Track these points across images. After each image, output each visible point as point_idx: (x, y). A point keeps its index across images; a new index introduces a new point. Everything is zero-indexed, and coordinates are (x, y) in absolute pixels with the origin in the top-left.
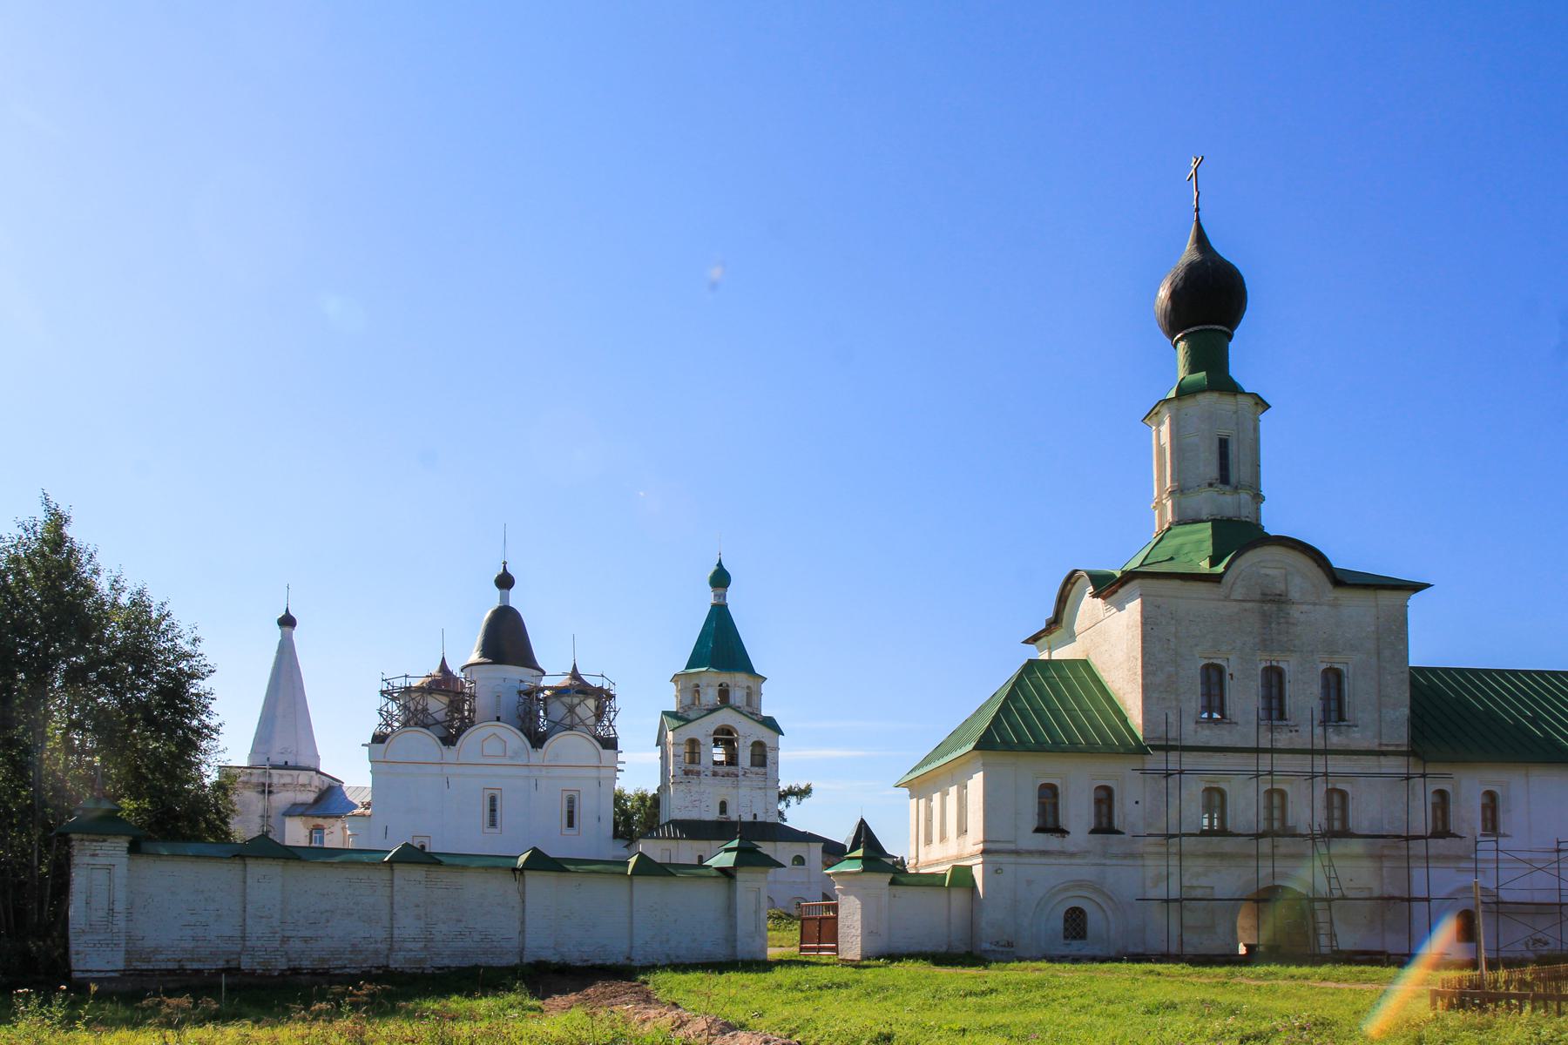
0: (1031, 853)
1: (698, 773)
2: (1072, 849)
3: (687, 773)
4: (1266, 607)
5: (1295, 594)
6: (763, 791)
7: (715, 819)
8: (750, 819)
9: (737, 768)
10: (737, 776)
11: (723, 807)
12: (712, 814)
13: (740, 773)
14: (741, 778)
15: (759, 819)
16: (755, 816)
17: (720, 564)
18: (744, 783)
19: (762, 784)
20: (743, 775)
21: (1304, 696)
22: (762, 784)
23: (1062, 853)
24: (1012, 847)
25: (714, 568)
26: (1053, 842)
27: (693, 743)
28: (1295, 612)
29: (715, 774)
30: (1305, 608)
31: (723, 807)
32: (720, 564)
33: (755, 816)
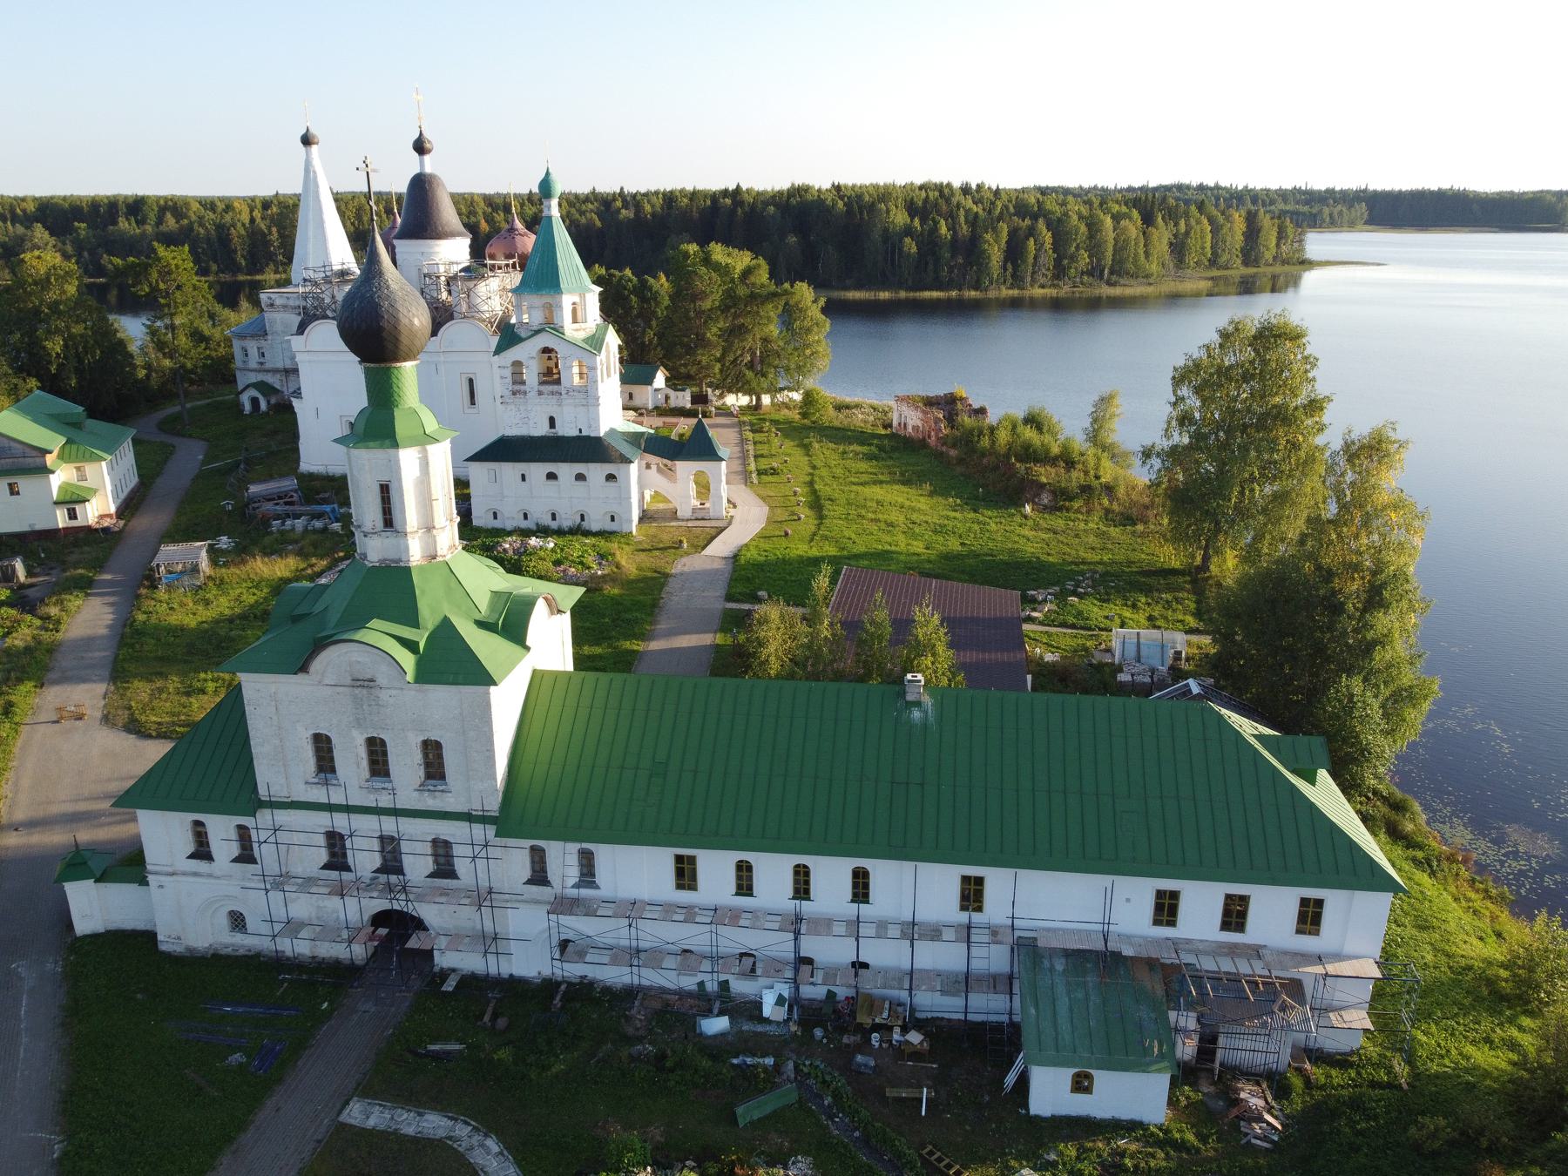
0: (184, 874)
1: (525, 393)
2: (218, 873)
3: (514, 393)
4: (357, 691)
5: (382, 680)
8: (577, 433)
11: (552, 422)
12: (540, 429)
14: (564, 396)
15: (584, 434)
16: (580, 431)
19: (584, 402)
21: (406, 765)
22: (584, 402)
23: (210, 876)
24: (170, 870)
26: (200, 866)
27: (517, 364)
28: (384, 695)
29: (540, 393)
30: (394, 692)
31: (552, 422)
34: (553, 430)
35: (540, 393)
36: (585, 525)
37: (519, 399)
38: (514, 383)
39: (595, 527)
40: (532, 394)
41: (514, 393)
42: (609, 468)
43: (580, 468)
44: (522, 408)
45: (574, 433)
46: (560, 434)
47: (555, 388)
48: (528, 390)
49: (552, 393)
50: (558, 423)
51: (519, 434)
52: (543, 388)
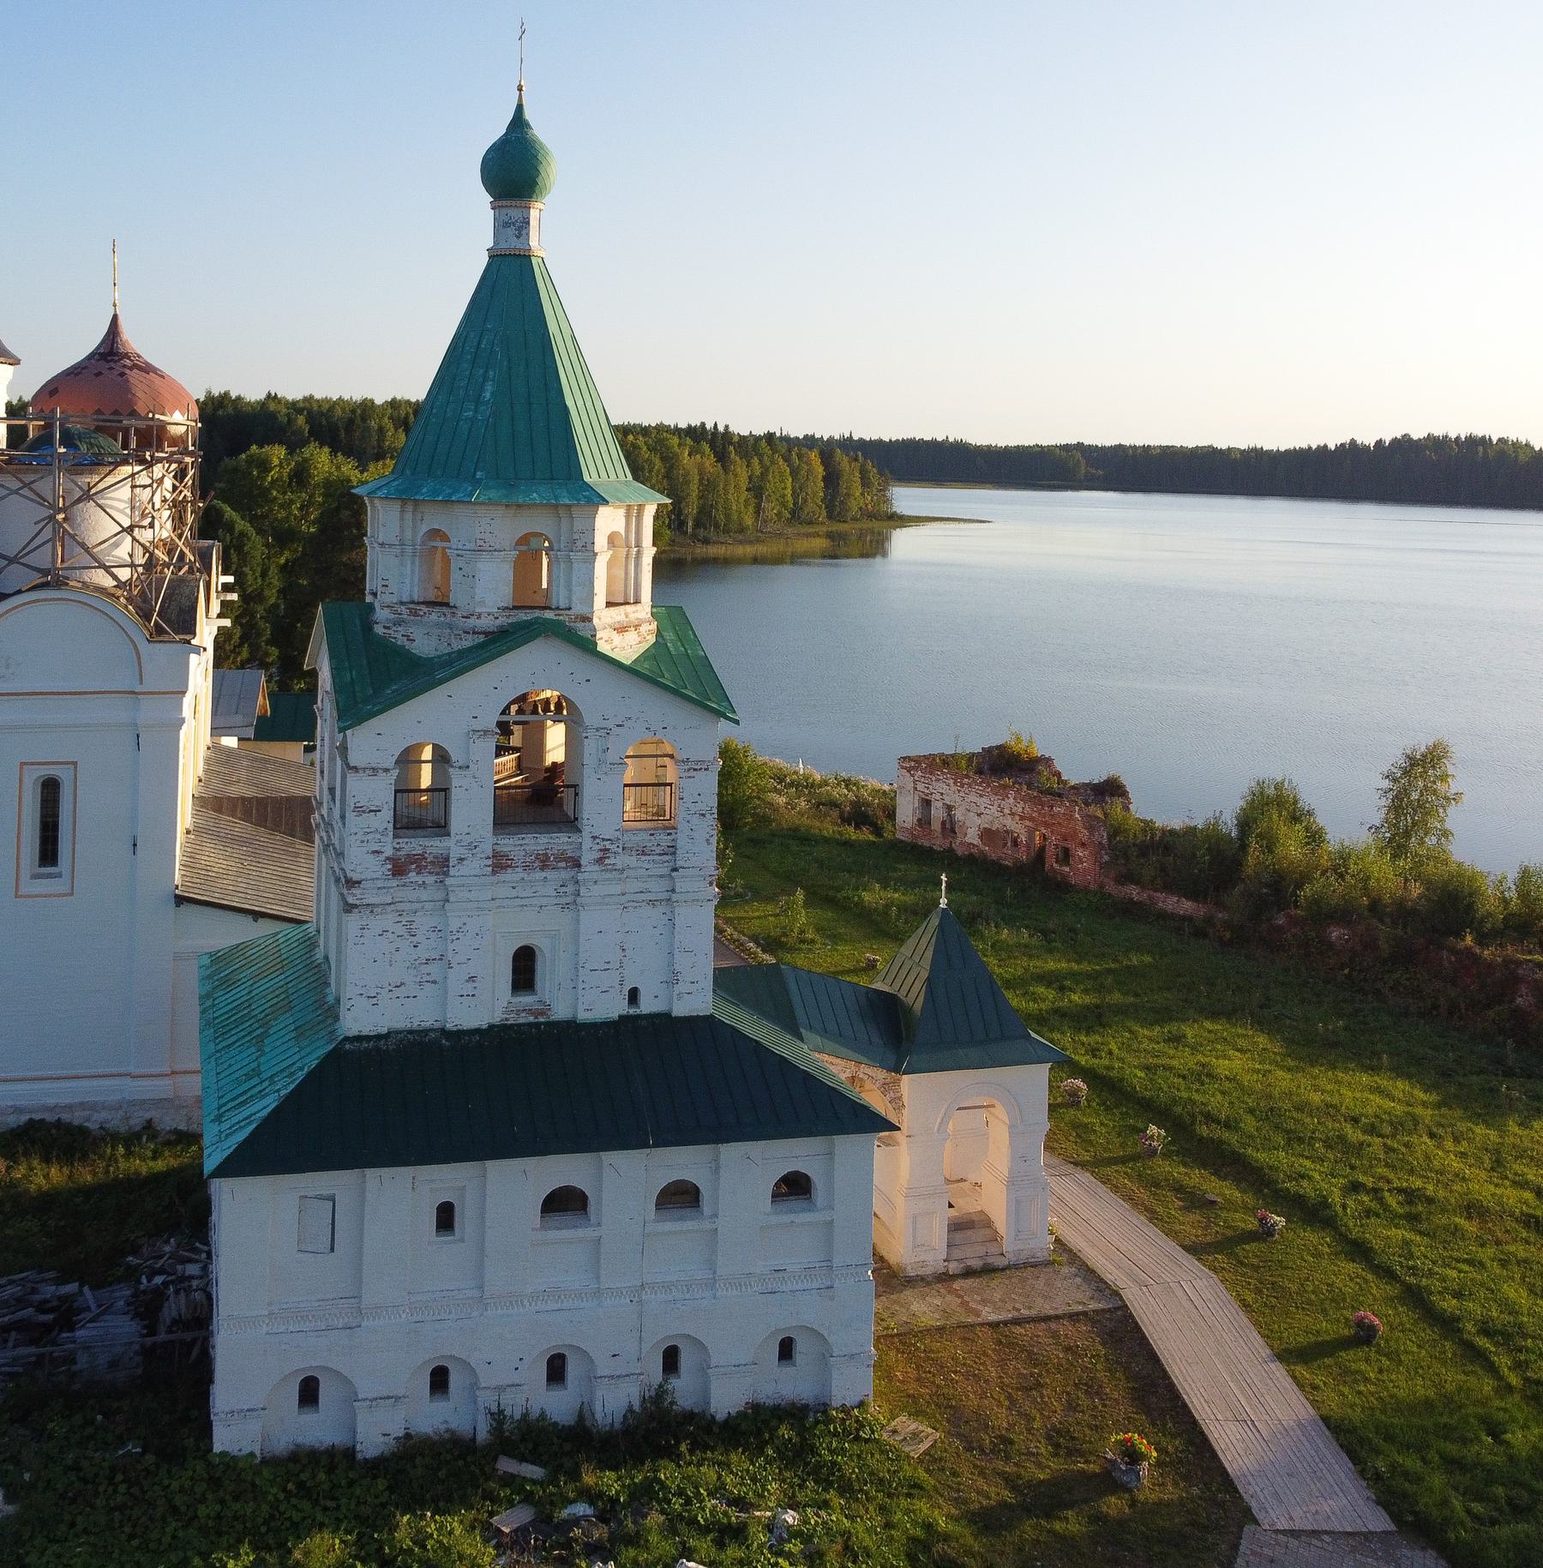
1: (442, 865)
6: (661, 909)
7: (497, 1017)
9: (574, 838)
10: (576, 864)
11: (524, 966)
13: (587, 858)
14: (589, 870)
17: (518, 122)
18: (598, 890)
20: (600, 861)
25: (499, 130)
29: (500, 863)
31: (524, 966)
32: (518, 122)
33: (633, 996)
35: (500, 863)
36: (684, 1392)
37: (419, 889)
39: (726, 1400)
41: (399, 868)
42: (794, 1154)
44: (424, 922)
45: (612, 1007)
47: (559, 841)
49: (544, 862)
50: (547, 975)
51: (401, 1024)
52: (512, 844)
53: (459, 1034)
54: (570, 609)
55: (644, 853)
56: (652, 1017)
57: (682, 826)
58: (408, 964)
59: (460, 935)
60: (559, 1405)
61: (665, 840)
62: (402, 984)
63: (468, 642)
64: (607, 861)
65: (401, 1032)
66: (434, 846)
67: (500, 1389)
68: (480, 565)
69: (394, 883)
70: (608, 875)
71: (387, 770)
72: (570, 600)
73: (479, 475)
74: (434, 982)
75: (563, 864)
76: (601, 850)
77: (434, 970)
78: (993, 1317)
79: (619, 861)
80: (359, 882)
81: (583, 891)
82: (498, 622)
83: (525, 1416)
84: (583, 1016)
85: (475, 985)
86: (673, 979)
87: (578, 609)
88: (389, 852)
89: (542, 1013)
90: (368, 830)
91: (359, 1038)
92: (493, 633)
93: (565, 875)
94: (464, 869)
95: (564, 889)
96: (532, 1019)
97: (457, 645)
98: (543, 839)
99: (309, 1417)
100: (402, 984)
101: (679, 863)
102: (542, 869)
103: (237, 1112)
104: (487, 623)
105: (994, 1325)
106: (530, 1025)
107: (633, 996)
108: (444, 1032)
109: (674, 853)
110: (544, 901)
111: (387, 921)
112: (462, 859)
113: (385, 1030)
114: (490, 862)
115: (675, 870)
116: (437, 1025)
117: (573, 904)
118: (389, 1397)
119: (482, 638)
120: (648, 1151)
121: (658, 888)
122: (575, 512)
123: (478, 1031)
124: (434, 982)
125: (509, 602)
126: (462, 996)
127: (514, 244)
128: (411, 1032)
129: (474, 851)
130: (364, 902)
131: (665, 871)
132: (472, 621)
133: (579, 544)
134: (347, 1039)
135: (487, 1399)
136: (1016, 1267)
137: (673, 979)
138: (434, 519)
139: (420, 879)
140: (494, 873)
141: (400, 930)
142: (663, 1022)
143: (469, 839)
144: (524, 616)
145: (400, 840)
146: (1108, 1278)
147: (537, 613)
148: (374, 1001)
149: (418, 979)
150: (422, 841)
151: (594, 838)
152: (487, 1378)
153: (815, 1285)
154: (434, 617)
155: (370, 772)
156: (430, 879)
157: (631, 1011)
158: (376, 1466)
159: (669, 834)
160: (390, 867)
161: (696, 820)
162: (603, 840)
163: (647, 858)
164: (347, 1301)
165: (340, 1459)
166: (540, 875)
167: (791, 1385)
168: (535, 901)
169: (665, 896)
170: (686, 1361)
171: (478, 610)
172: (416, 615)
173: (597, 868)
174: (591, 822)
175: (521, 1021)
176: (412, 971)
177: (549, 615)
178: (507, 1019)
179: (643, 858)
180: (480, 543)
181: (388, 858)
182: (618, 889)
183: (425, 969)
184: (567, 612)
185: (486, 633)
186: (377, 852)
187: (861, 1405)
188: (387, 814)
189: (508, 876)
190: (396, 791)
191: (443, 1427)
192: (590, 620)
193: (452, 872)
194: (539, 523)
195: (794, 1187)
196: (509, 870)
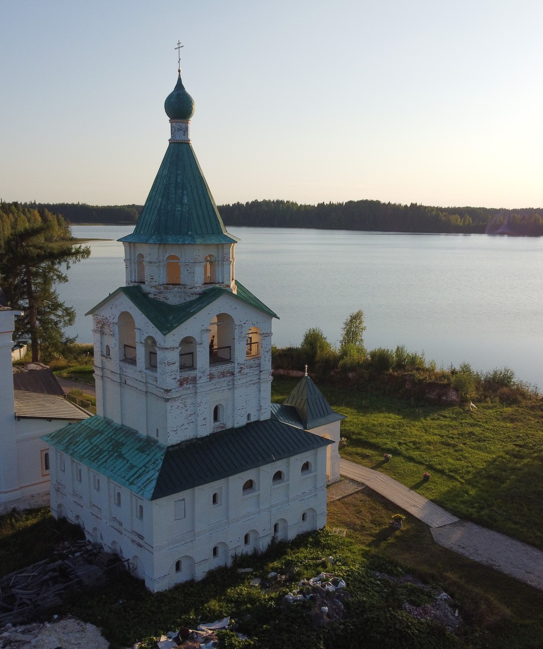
3: (181, 384)
10: (233, 374)
13: (237, 371)
14: (237, 374)
15: (253, 419)
20: (240, 372)
29: (211, 377)
33: (249, 416)
34: (217, 424)
35: (211, 377)
36: (280, 536)
38: (183, 367)
39: (292, 535)
40: (203, 380)
43: (279, 466)
44: (189, 401)
45: (241, 422)
46: (229, 426)
47: (226, 367)
48: (199, 375)
49: (223, 375)
51: (184, 439)
53: (202, 439)
54: (223, 283)
55: (251, 368)
56: (254, 422)
57: (263, 357)
58: (185, 417)
59: (201, 404)
60: (248, 549)
61: (257, 362)
62: (183, 425)
63: (194, 298)
64: (242, 372)
65: (184, 441)
66: (192, 373)
67: (235, 548)
68: (196, 268)
69: (181, 389)
70: (242, 376)
71: (177, 348)
72: (223, 279)
73: (189, 233)
74: (193, 422)
75: (229, 375)
76: (240, 368)
77: (192, 418)
78: (337, 498)
79: (245, 371)
80: (170, 390)
81: (236, 383)
82: (202, 289)
83: (242, 554)
84: (236, 426)
85: (205, 421)
86: (260, 409)
87: (226, 283)
88: (178, 378)
89: (223, 427)
90: (171, 371)
91: (172, 446)
92: (201, 294)
93: (230, 378)
94: (201, 381)
95: (229, 383)
96: (221, 430)
97: (188, 299)
98: (224, 366)
99: (179, 574)
100: (183, 425)
101: (261, 369)
102: (223, 377)
103: (139, 479)
104: (199, 290)
105: (339, 500)
106: (221, 431)
107: (249, 416)
108: (197, 439)
109: (259, 366)
110: (224, 388)
111: (178, 403)
112: (201, 377)
113: (180, 442)
114: (209, 377)
115: (261, 372)
116: (194, 437)
117: (233, 388)
118: (205, 560)
119: (198, 296)
120: (274, 463)
121: (255, 378)
122: (225, 246)
123: (207, 436)
124: (193, 422)
125: (203, 283)
126: (202, 425)
127: (180, 138)
128: (187, 441)
129: (204, 374)
130: (172, 397)
131: (258, 372)
132: (193, 290)
133: (226, 258)
134: (168, 447)
135: (231, 553)
136: (335, 483)
137: (260, 409)
138: (173, 251)
139: (188, 386)
140: (210, 381)
141: (182, 405)
142: (257, 422)
143: (202, 370)
144: (210, 287)
145: (182, 373)
146: (358, 480)
147: (214, 285)
148: (176, 432)
149: (188, 422)
150: (189, 372)
151: (238, 364)
152: (231, 546)
153: (313, 495)
154: (176, 289)
155: (172, 349)
156: (191, 386)
157: (248, 422)
158: (204, 581)
159: (259, 360)
160: (179, 383)
161: (266, 354)
162: (241, 364)
163: (252, 369)
164: (190, 533)
165: (191, 583)
166: (223, 379)
167: (306, 527)
168: (220, 389)
169: (257, 381)
170: (280, 527)
171: (196, 285)
172: (167, 289)
173: (239, 374)
174: (237, 359)
175: (218, 431)
176: (186, 420)
177: (217, 286)
178: (214, 431)
179: (251, 369)
180: (195, 260)
181: (178, 380)
182: (245, 381)
183: (190, 418)
184: (223, 284)
185: (199, 294)
186: (175, 378)
187: (324, 527)
188: (177, 364)
189: (214, 381)
190: (180, 355)
191: (217, 566)
192: (229, 286)
193: (198, 382)
194: (213, 251)
195: (306, 467)
196: (213, 379)
